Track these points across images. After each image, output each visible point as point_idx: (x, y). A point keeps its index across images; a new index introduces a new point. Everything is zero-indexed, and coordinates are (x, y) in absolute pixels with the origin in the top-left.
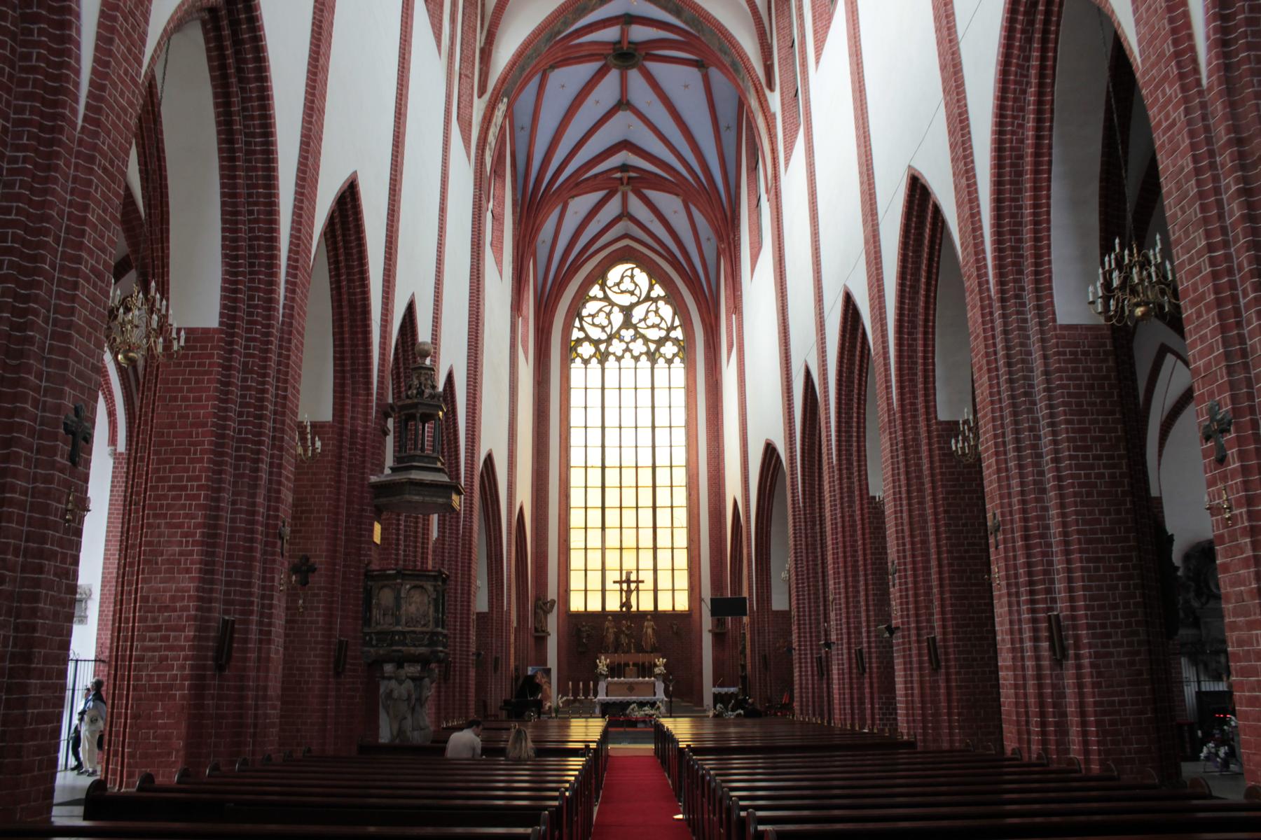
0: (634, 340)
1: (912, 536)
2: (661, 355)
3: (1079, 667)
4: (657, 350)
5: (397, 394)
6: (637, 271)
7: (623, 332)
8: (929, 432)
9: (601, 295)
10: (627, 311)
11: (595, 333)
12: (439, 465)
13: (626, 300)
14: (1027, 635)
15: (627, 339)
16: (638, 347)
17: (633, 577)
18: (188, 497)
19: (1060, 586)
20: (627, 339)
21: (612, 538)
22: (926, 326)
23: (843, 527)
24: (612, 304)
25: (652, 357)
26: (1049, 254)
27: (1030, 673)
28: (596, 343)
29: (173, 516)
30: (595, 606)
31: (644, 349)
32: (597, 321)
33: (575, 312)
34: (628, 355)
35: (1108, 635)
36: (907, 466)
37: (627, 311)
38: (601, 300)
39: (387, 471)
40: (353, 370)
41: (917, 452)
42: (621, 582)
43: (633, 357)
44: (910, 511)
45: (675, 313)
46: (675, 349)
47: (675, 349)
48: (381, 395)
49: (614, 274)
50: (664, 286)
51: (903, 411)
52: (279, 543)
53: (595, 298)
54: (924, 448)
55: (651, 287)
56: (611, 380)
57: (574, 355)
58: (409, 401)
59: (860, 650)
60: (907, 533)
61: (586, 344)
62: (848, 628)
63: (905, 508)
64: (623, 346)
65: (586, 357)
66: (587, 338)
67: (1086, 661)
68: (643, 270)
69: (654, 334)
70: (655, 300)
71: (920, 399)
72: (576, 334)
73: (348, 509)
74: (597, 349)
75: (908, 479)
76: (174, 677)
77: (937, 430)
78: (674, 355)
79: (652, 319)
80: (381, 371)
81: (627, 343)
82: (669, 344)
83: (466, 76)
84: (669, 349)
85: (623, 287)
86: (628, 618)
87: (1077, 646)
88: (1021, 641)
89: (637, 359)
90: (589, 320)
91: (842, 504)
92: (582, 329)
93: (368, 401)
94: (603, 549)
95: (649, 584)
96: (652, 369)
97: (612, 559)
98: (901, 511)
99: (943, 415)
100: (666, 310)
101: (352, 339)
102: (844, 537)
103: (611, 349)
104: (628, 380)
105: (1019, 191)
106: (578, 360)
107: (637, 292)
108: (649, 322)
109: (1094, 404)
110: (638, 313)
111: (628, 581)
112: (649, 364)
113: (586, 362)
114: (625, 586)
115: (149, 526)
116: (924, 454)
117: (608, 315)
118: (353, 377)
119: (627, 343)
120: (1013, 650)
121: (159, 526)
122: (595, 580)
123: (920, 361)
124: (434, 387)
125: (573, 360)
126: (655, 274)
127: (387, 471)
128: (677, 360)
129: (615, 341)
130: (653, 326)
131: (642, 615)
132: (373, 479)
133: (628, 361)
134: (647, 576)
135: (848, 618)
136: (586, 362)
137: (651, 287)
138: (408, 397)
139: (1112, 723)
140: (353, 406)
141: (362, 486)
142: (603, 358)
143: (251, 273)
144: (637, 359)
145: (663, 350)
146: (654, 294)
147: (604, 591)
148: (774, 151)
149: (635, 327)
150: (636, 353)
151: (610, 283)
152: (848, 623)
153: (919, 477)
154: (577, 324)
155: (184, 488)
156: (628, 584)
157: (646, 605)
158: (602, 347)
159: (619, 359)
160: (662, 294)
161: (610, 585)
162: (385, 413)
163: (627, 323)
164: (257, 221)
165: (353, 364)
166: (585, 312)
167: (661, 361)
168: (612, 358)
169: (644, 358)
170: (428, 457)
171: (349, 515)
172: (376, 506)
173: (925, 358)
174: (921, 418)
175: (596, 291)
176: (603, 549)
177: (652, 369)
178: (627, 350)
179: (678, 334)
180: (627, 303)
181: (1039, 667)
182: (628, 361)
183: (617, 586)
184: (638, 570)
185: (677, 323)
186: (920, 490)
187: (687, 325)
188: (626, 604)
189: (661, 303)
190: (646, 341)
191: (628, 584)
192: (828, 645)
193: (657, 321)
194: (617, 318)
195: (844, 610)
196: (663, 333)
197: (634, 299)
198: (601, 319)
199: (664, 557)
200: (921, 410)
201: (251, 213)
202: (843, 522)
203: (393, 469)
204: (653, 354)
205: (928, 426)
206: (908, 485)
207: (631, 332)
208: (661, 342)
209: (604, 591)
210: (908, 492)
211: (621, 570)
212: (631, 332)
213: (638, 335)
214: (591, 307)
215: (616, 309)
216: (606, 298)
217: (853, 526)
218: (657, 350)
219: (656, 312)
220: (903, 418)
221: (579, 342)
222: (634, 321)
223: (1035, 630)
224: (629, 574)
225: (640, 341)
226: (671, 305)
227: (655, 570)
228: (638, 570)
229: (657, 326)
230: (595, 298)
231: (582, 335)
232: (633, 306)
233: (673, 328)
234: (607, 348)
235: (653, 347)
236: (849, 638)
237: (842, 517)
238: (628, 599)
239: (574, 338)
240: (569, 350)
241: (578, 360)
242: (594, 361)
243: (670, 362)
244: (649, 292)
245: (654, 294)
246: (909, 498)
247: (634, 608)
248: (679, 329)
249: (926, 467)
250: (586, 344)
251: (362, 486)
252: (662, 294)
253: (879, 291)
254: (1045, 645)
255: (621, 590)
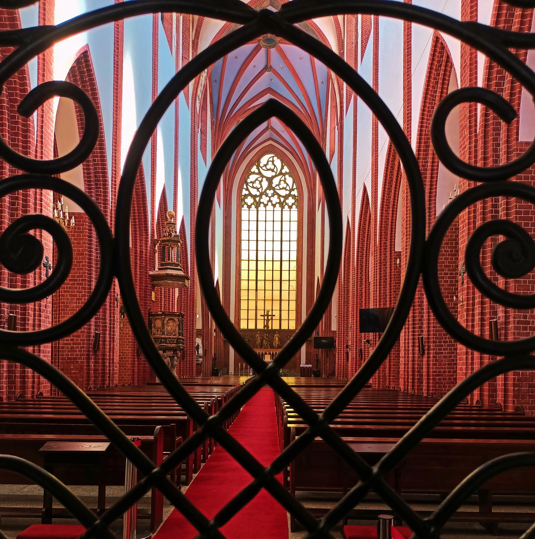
0: (273, 195)
1: (380, 302)
2: (286, 204)
3: (429, 357)
4: (285, 201)
5: (159, 236)
6: (275, 158)
7: (268, 191)
8: (391, 256)
9: (257, 171)
10: (270, 180)
11: (254, 192)
12: (179, 268)
13: (269, 174)
14: (410, 345)
15: (270, 195)
16: (275, 199)
17: (270, 313)
18: (78, 284)
19: (425, 325)
20: (270, 195)
21: (261, 294)
22: (393, 208)
23: (357, 295)
24: (263, 176)
25: (282, 205)
26: (436, 185)
27: (410, 359)
28: (254, 197)
29: (72, 292)
30: (252, 326)
31: (278, 201)
32: (255, 185)
33: (244, 180)
34: (270, 204)
35: (442, 346)
36: (380, 271)
37: (270, 180)
38: (257, 174)
39: (157, 269)
40: (139, 224)
41: (385, 265)
42: (264, 316)
43: (272, 205)
44: (380, 291)
45: (294, 182)
46: (293, 201)
47: (293, 201)
48: (153, 235)
49: (264, 160)
50: (289, 167)
51: (380, 247)
52: (116, 302)
53: (254, 173)
54: (388, 263)
55: (282, 168)
56: (261, 217)
57: (243, 203)
58: (165, 238)
59: (361, 350)
60: (378, 300)
61: (249, 197)
62: (356, 340)
63: (378, 289)
64: (268, 199)
65: (249, 204)
66: (250, 194)
67: (431, 355)
68: (278, 158)
69: (283, 193)
70: (284, 175)
71: (389, 241)
72: (244, 192)
73: (140, 286)
74: (255, 200)
75: (380, 277)
76: (77, 355)
77: (394, 255)
78: (293, 204)
79: (283, 185)
80: (152, 225)
81: (270, 197)
82: (290, 198)
83: (186, 58)
84: (290, 201)
85: (268, 167)
86: (268, 332)
87: (429, 349)
88: (408, 347)
89: (274, 206)
90: (251, 185)
91: (357, 285)
92: (247, 189)
93: (147, 238)
94: (256, 300)
95: (277, 316)
96: (282, 211)
97: (260, 305)
98: (376, 291)
99: (397, 250)
100: (290, 180)
101: (138, 210)
102: (357, 300)
103: (262, 200)
104: (270, 217)
105: (427, 154)
106: (245, 206)
107: (275, 170)
108: (281, 186)
109: (448, 251)
110: (276, 181)
111: (268, 315)
112: (280, 209)
113: (249, 207)
114: (266, 318)
115: (63, 295)
116: (388, 266)
117: (260, 182)
118: (140, 227)
119: (270, 197)
120: (405, 350)
121: (67, 296)
122: (252, 314)
123: (390, 224)
124: (176, 232)
125: (243, 206)
126: (285, 161)
127: (157, 269)
128: (294, 207)
129: (264, 196)
130: (283, 189)
131: (274, 331)
132: (151, 273)
133: (270, 207)
134: (276, 313)
135: (356, 335)
136: (249, 207)
137: (282, 168)
138: (164, 236)
139: (439, 379)
140: (140, 240)
141: (146, 276)
142: (257, 205)
143: (96, 188)
144: (274, 206)
145: (287, 201)
146: (284, 171)
147: (256, 319)
148: (341, 103)
149: (274, 189)
150: (274, 203)
151: (261, 165)
152: (356, 337)
153: (385, 276)
154: (245, 187)
155: (76, 280)
156: (268, 317)
157: (276, 326)
158: (257, 199)
159: (265, 206)
160: (288, 171)
161: (259, 317)
162: (154, 243)
163: (270, 187)
164: (98, 164)
165: (139, 221)
166: (249, 181)
167: (286, 207)
168: (262, 205)
169: (278, 205)
170: (174, 264)
171: (140, 289)
172: (152, 285)
173: (392, 223)
174: (388, 250)
175: (254, 169)
176: (256, 300)
177: (282, 211)
178: (270, 201)
179: (295, 193)
180: (270, 176)
181: (414, 357)
182: (270, 207)
183: (263, 318)
184: (272, 310)
185: (295, 187)
186: (385, 282)
187: (300, 189)
188: (266, 326)
189: (287, 176)
190: (279, 196)
191: (268, 317)
192: (347, 347)
193: (285, 185)
194: (265, 184)
195: (355, 332)
196: (288, 192)
197: (274, 174)
198: (257, 184)
199: (285, 305)
200: (388, 247)
201: (94, 161)
202: (357, 293)
203: (159, 269)
204: (283, 203)
205: (391, 253)
206: (380, 279)
207: (272, 191)
208: (286, 197)
209: (256, 319)
210: (380, 282)
211: (264, 310)
212: (272, 191)
213: (275, 193)
214: (252, 178)
215: (264, 179)
216: (260, 173)
217: (361, 295)
218: (285, 201)
219: (285, 181)
220: (380, 250)
221: (246, 196)
222: (274, 185)
223: (414, 343)
224: (268, 311)
225: (276, 196)
226: (292, 177)
227: (280, 310)
228: (272, 310)
229: (285, 188)
230: (254, 173)
231: (247, 193)
232: (273, 177)
233: (293, 190)
234: (260, 200)
235: (282, 199)
236: (356, 344)
237: (357, 291)
238: (268, 324)
239: (243, 194)
240: (241, 200)
241: (245, 206)
242: (253, 206)
243: (290, 207)
244: (281, 170)
245: (284, 171)
246: (380, 285)
247: (270, 328)
248: (296, 190)
249: (388, 271)
250: (249, 197)
251: (146, 276)
252: (288, 171)
253: (375, 189)
254: (417, 349)
255: (264, 319)
